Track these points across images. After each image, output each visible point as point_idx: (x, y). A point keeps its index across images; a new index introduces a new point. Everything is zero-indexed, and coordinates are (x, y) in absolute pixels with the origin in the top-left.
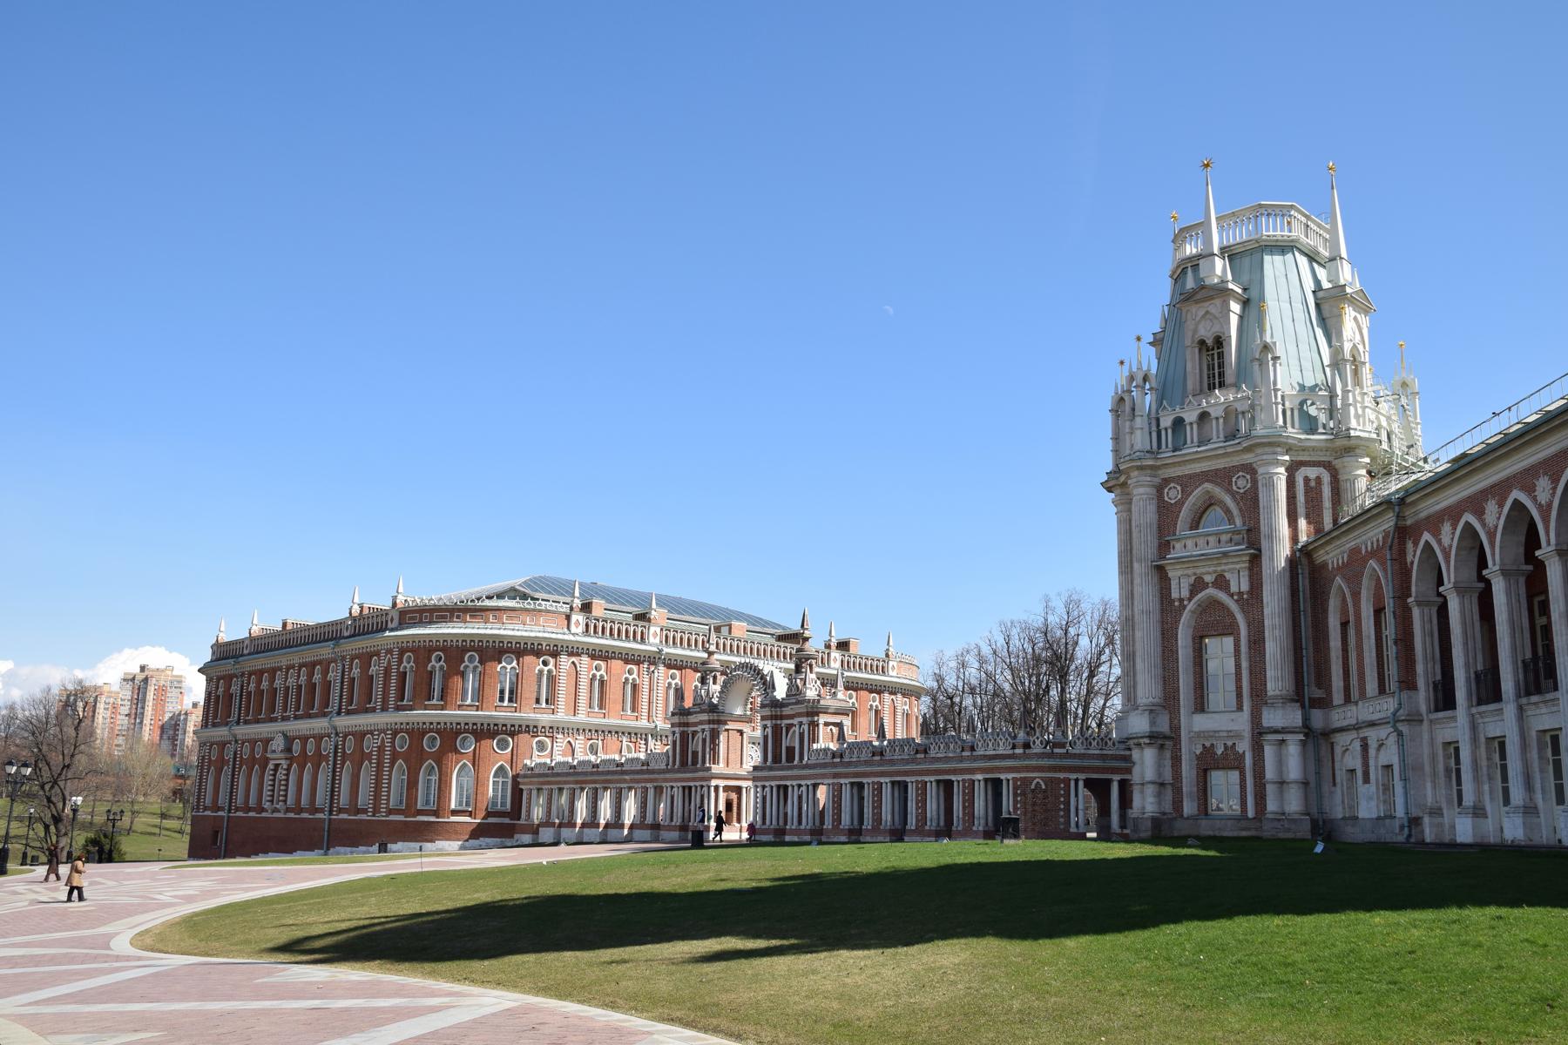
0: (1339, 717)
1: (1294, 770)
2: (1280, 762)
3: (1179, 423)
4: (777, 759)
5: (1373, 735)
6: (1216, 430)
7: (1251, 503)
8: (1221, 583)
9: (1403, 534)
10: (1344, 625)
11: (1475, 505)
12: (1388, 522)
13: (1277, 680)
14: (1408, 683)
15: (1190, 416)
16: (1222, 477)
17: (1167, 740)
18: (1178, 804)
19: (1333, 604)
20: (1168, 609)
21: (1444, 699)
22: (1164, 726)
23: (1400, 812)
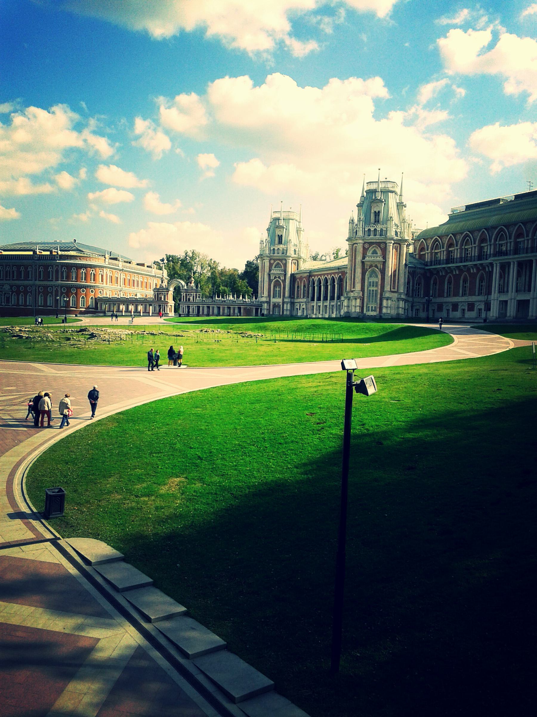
0: (296, 301)
1: (289, 308)
2: (287, 307)
3: (274, 249)
4: (186, 300)
5: (302, 304)
6: (280, 252)
7: (285, 265)
8: (279, 278)
9: (310, 276)
10: (298, 287)
11: (321, 275)
12: (308, 274)
13: (287, 294)
14: (308, 297)
15: (276, 249)
16: (281, 260)
17: (268, 303)
18: (269, 312)
19: (296, 283)
20: (270, 281)
21: (313, 299)
22: (268, 300)
23: (305, 314)
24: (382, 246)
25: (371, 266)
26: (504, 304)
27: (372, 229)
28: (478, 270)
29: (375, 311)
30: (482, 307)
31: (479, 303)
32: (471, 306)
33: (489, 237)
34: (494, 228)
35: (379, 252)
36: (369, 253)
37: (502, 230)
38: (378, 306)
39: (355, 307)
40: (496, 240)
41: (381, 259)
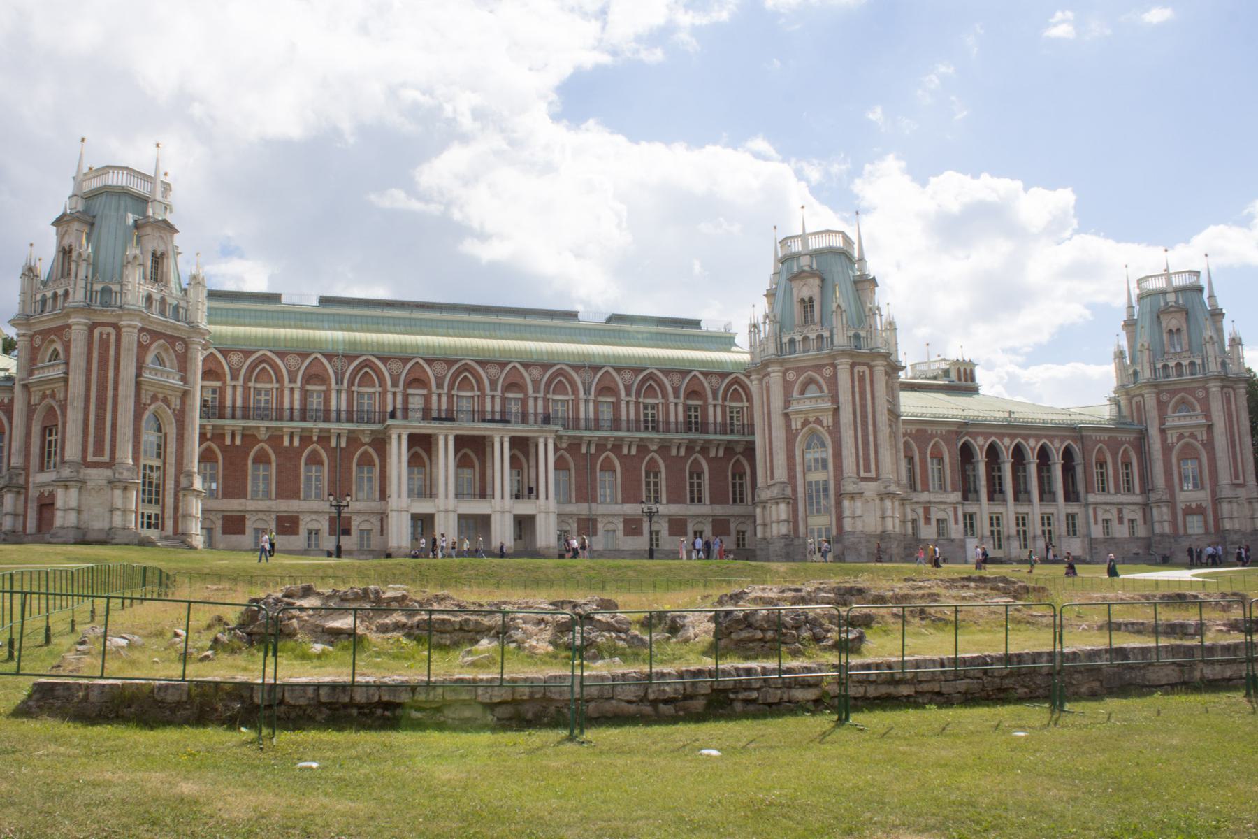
24: (179, 347)
25: (154, 398)
26: (423, 523)
27: (156, 296)
28: (306, 439)
29: (156, 526)
30: (324, 526)
31: (314, 517)
32: (288, 525)
33: (336, 374)
34: (350, 358)
35: (170, 359)
36: (150, 358)
37: (367, 364)
38: (169, 512)
39: (125, 511)
40: (351, 383)
41: (176, 382)
